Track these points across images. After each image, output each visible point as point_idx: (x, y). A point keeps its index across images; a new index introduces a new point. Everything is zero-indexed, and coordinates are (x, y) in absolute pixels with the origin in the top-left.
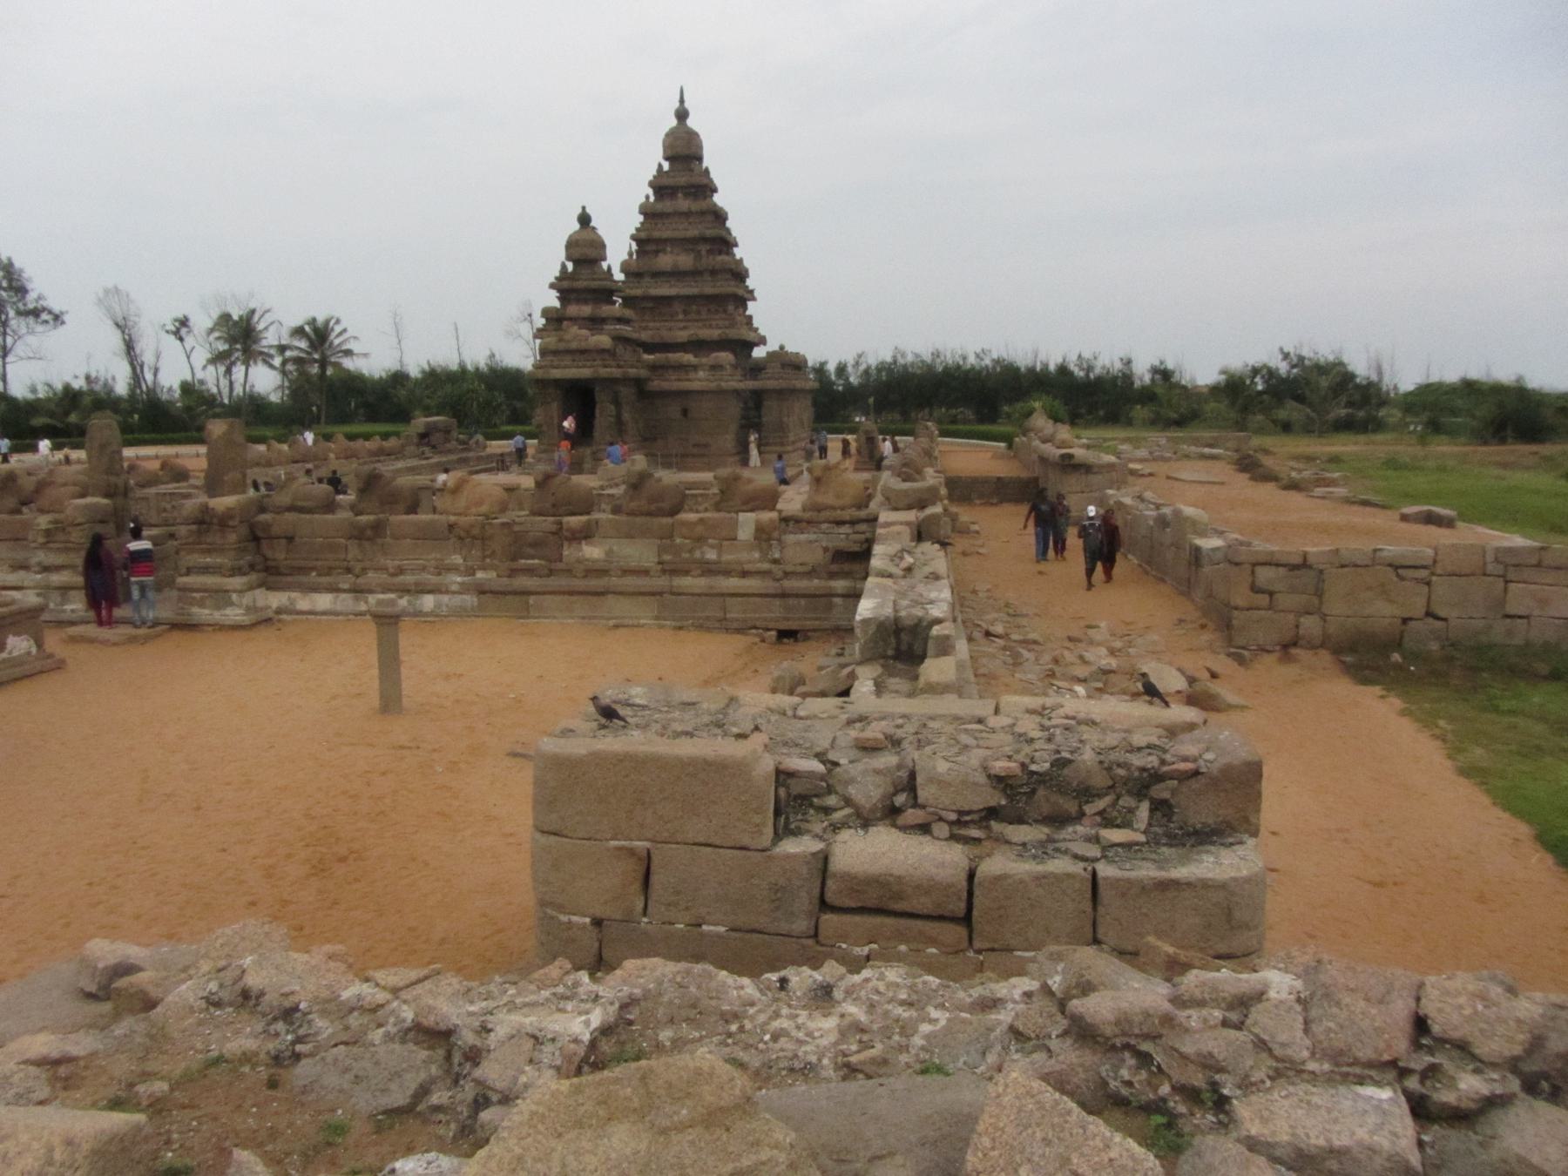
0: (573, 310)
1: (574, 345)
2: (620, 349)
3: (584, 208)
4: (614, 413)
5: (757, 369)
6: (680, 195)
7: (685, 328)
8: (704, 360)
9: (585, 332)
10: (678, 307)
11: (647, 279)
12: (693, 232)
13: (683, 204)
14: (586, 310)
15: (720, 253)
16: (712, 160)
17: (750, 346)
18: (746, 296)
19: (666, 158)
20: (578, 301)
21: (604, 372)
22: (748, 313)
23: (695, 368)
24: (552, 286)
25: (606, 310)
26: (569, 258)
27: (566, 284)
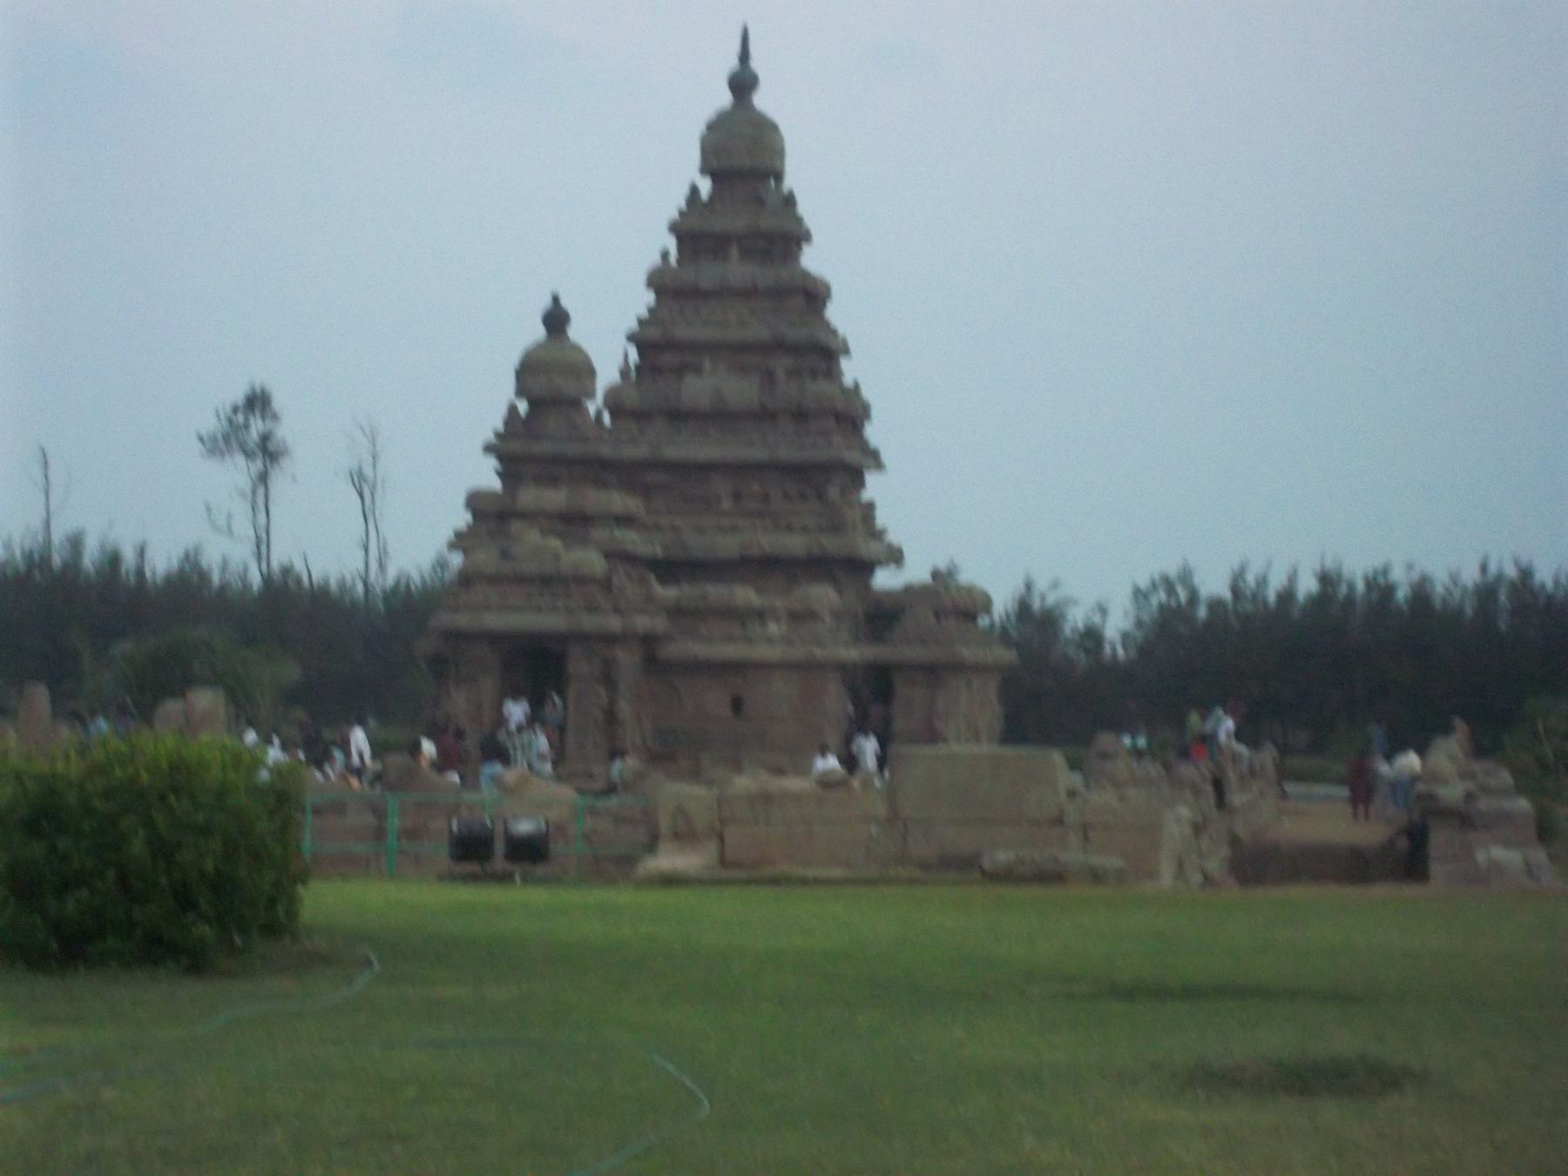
0: (530, 497)
1: (530, 567)
2: (620, 579)
3: (556, 300)
6: (734, 252)
8: (779, 603)
9: (555, 543)
10: (722, 487)
12: (757, 331)
13: (737, 270)
14: (555, 498)
15: (814, 374)
17: (864, 568)
19: (705, 169)
20: (538, 480)
21: (589, 623)
23: (761, 615)
24: (488, 449)
27: (516, 446)
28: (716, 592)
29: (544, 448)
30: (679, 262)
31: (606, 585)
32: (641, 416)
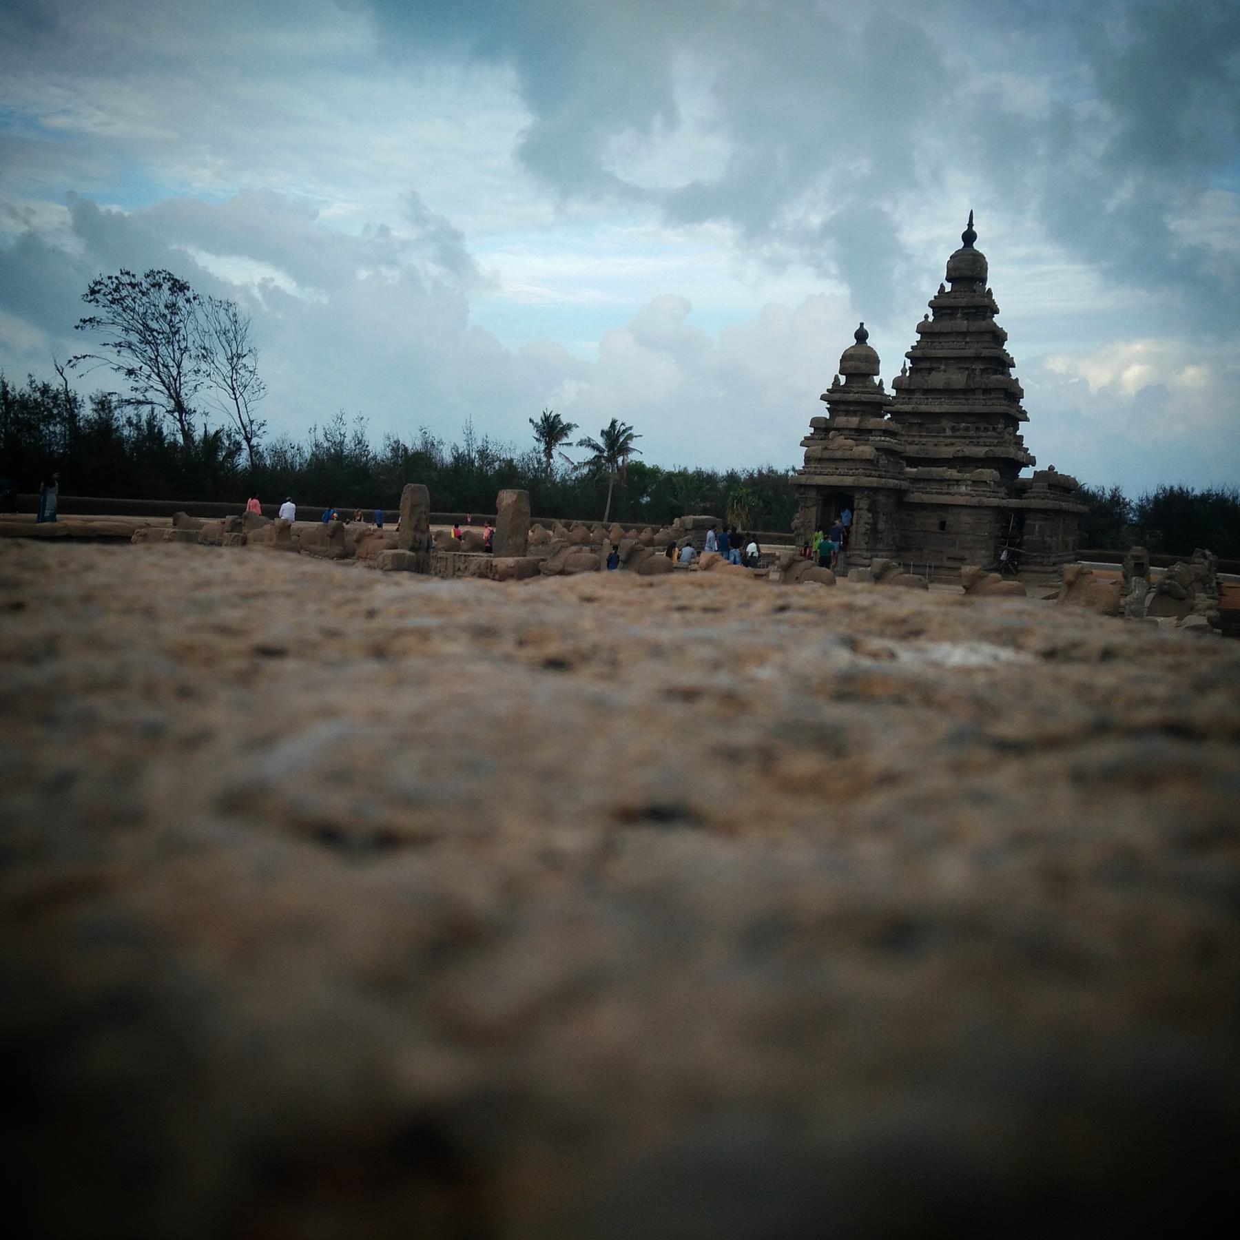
0: (841, 421)
1: (838, 454)
3: (862, 324)
4: (871, 521)
5: (1022, 489)
6: (959, 315)
7: (952, 444)
8: (967, 476)
9: (850, 442)
11: (918, 395)
12: (970, 352)
13: (961, 324)
14: (854, 421)
15: (995, 372)
16: (998, 283)
18: (1020, 416)
20: (847, 413)
21: (866, 481)
22: (1018, 433)
24: (823, 398)
25: (872, 422)
26: (841, 373)
27: (837, 396)
28: (937, 471)
29: (851, 397)
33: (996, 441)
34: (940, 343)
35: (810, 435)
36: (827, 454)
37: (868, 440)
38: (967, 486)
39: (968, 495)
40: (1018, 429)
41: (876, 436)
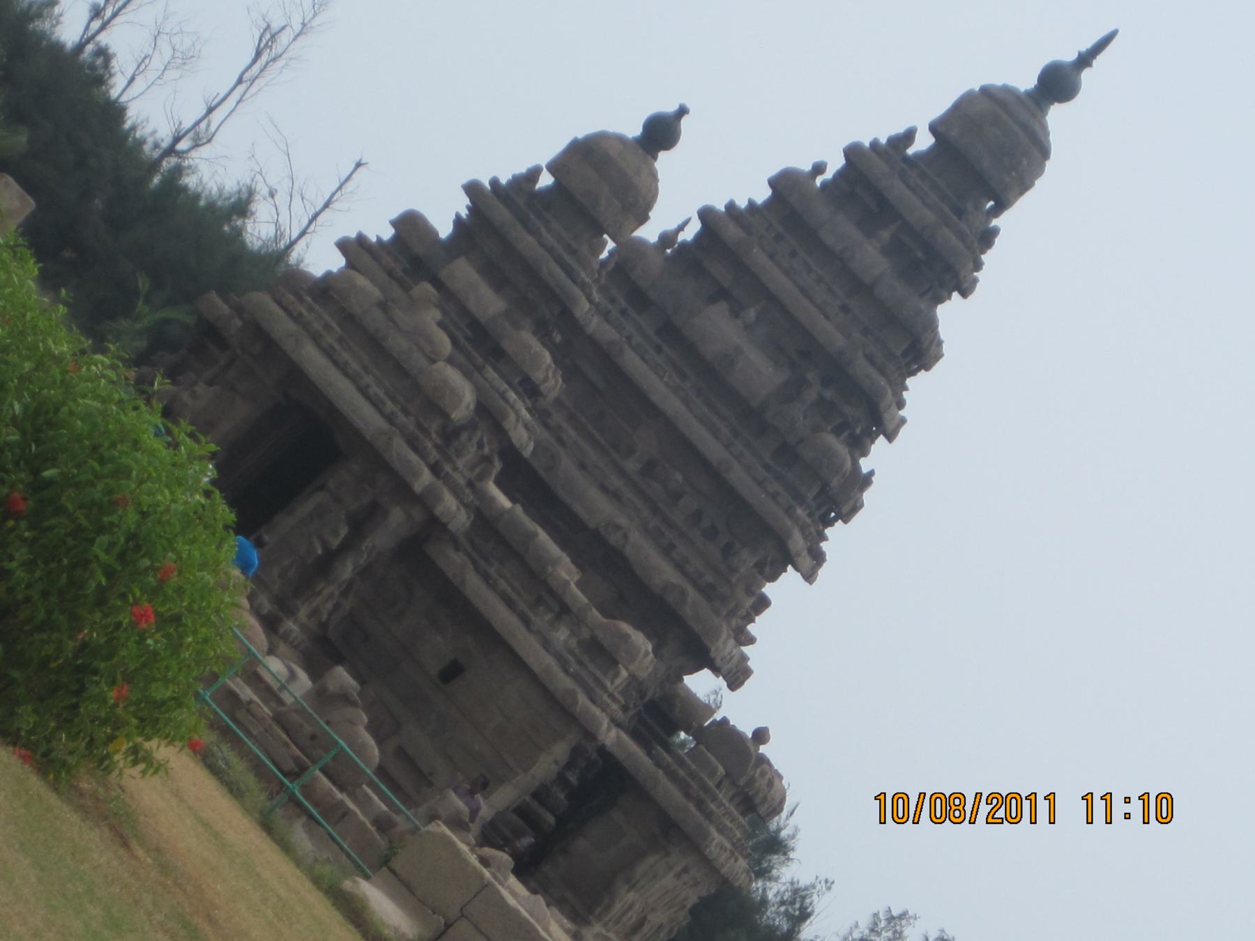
0: (463, 273)
1: (397, 343)
3: (682, 111)
4: (335, 543)
6: (885, 235)
7: (616, 496)
12: (830, 333)
22: (769, 589)
24: (472, 189)
26: (554, 167)
29: (526, 243)
30: (825, 185)
31: (450, 434)
32: (639, 298)
33: (709, 578)
34: (793, 254)
35: (374, 239)
36: (376, 320)
37: (480, 369)
38: (573, 634)
39: (559, 657)
40: (773, 577)
41: (503, 376)
